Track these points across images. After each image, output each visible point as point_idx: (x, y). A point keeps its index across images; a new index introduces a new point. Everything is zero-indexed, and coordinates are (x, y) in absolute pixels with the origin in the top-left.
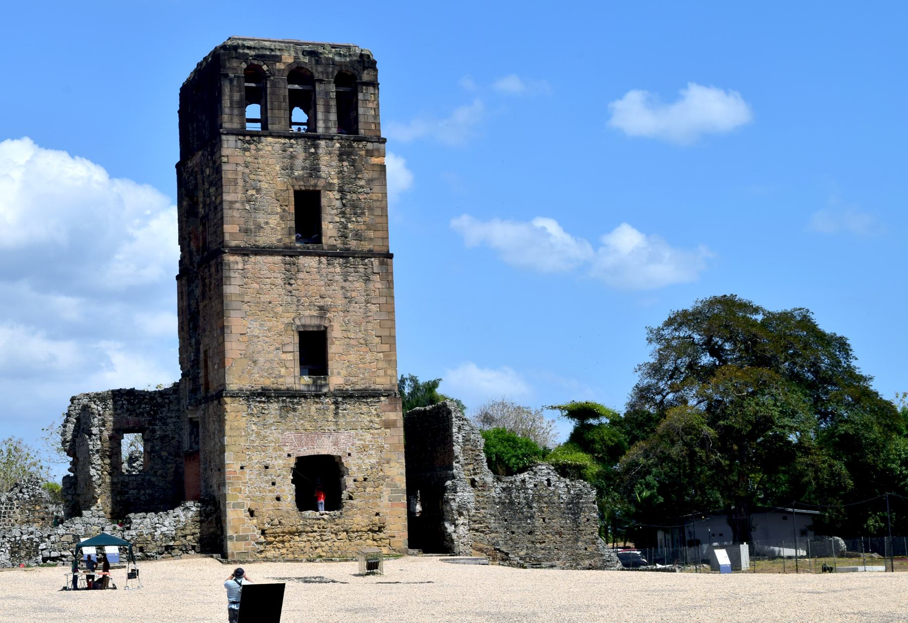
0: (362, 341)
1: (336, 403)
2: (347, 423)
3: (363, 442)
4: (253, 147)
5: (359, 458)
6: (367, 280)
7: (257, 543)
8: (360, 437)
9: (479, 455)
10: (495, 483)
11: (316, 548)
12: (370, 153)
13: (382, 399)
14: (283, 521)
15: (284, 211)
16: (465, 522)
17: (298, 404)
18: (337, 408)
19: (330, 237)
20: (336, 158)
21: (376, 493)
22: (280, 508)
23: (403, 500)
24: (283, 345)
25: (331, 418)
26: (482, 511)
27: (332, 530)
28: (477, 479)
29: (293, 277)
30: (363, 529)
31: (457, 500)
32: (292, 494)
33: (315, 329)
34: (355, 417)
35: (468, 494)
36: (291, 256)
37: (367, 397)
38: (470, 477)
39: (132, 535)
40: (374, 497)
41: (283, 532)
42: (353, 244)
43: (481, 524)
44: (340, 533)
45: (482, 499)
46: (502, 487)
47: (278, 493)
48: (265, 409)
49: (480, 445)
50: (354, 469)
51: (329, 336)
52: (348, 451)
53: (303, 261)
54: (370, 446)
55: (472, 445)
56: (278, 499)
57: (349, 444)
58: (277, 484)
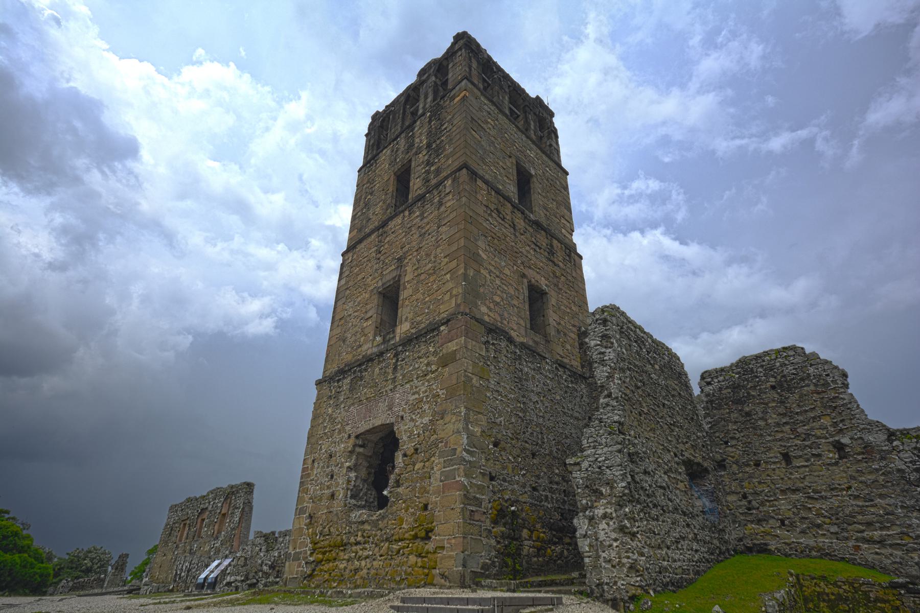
0: (431, 271)
1: (396, 355)
2: (404, 376)
3: (417, 396)
4: (375, 164)
5: (412, 420)
6: (441, 204)
7: (306, 563)
8: (415, 390)
9: (835, 398)
10: (895, 443)
11: (356, 570)
12: (453, 98)
13: (442, 328)
14: (332, 529)
15: (386, 194)
16: (609, 511)
17: (366, 370)
18: (397, 361)
19: (416, 190)
20: (427, 124)
21: (426, 470)
22: (331, 510)
23: (459, 476)
24: (366, 312)
25: (390, 376)
26: (878, 500)
27: (376, 539)
28: (845, 440)
29: (383, 244)
30: (407, 536)
31: (585, 465)
32: (343, 489)
33: (391, 283)
34: (411, 365)
35: (606, 449)
36: (383, 227)
37: (426, 333)
38: (831, 440)
39: (275, 557)
40: (422, 478)
41: (330, 546)
42: (434, 182)
43: (888, 528)
44: (382, 544)
45: (872, 477)
46: (915, 448)
47: (334, 489)
48: (340, 387)
49: (834, 382)
50: (405, 438)
51: (402, 283)
52: (401, 413)
53: (391, 224)
54: (425, 400)
55: (816, 385)
56: (333, 496)
57: (403, 403)
58: (335, 477)
